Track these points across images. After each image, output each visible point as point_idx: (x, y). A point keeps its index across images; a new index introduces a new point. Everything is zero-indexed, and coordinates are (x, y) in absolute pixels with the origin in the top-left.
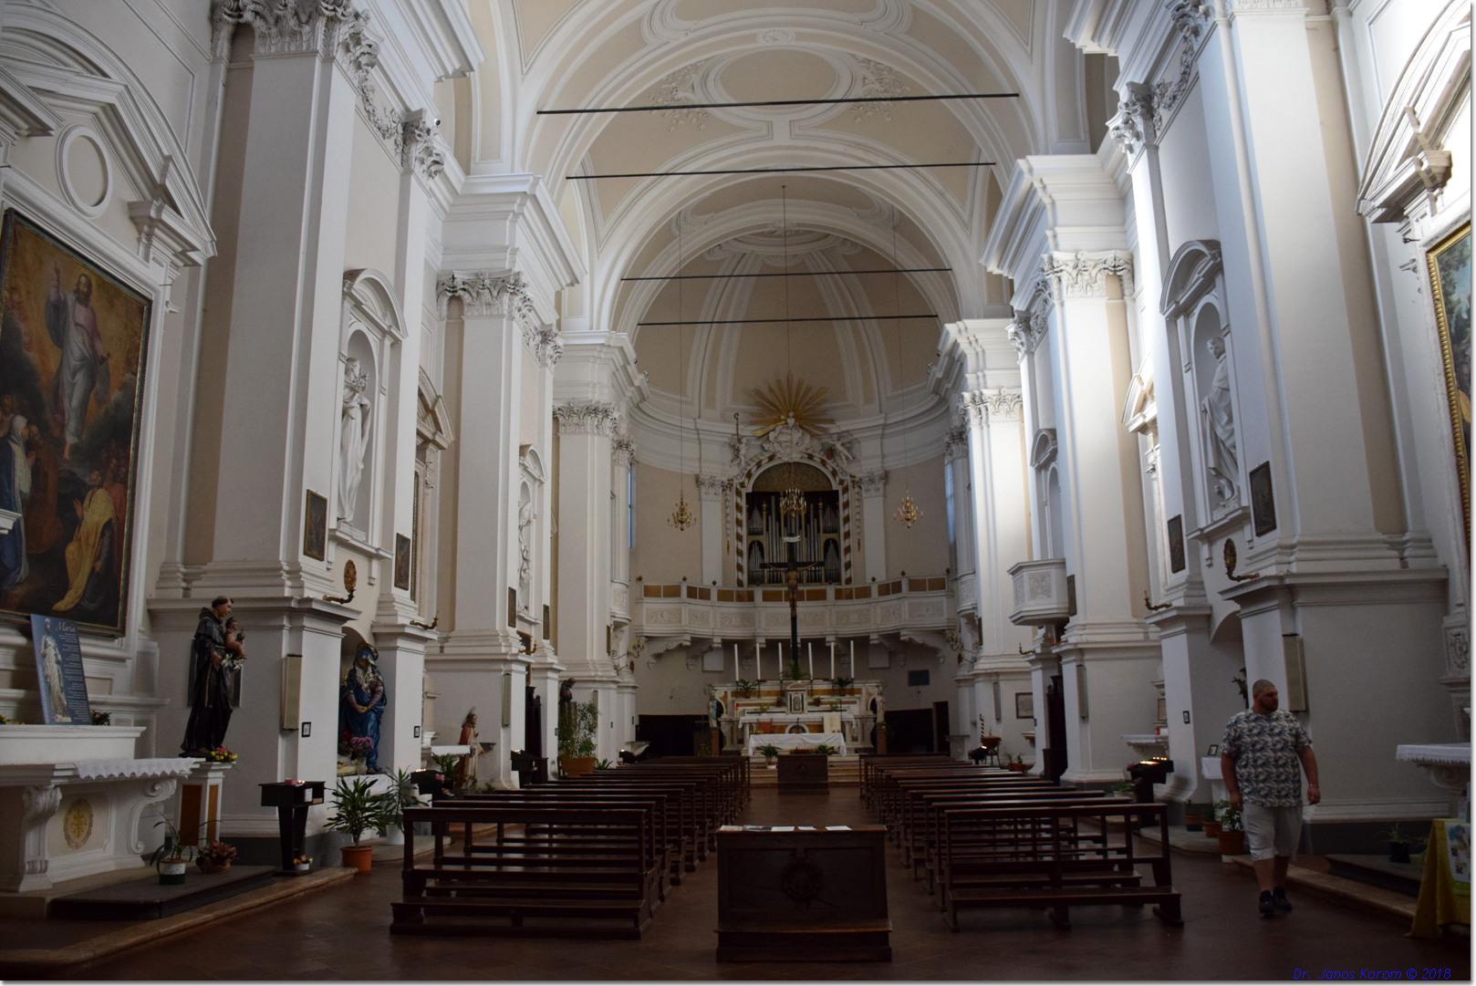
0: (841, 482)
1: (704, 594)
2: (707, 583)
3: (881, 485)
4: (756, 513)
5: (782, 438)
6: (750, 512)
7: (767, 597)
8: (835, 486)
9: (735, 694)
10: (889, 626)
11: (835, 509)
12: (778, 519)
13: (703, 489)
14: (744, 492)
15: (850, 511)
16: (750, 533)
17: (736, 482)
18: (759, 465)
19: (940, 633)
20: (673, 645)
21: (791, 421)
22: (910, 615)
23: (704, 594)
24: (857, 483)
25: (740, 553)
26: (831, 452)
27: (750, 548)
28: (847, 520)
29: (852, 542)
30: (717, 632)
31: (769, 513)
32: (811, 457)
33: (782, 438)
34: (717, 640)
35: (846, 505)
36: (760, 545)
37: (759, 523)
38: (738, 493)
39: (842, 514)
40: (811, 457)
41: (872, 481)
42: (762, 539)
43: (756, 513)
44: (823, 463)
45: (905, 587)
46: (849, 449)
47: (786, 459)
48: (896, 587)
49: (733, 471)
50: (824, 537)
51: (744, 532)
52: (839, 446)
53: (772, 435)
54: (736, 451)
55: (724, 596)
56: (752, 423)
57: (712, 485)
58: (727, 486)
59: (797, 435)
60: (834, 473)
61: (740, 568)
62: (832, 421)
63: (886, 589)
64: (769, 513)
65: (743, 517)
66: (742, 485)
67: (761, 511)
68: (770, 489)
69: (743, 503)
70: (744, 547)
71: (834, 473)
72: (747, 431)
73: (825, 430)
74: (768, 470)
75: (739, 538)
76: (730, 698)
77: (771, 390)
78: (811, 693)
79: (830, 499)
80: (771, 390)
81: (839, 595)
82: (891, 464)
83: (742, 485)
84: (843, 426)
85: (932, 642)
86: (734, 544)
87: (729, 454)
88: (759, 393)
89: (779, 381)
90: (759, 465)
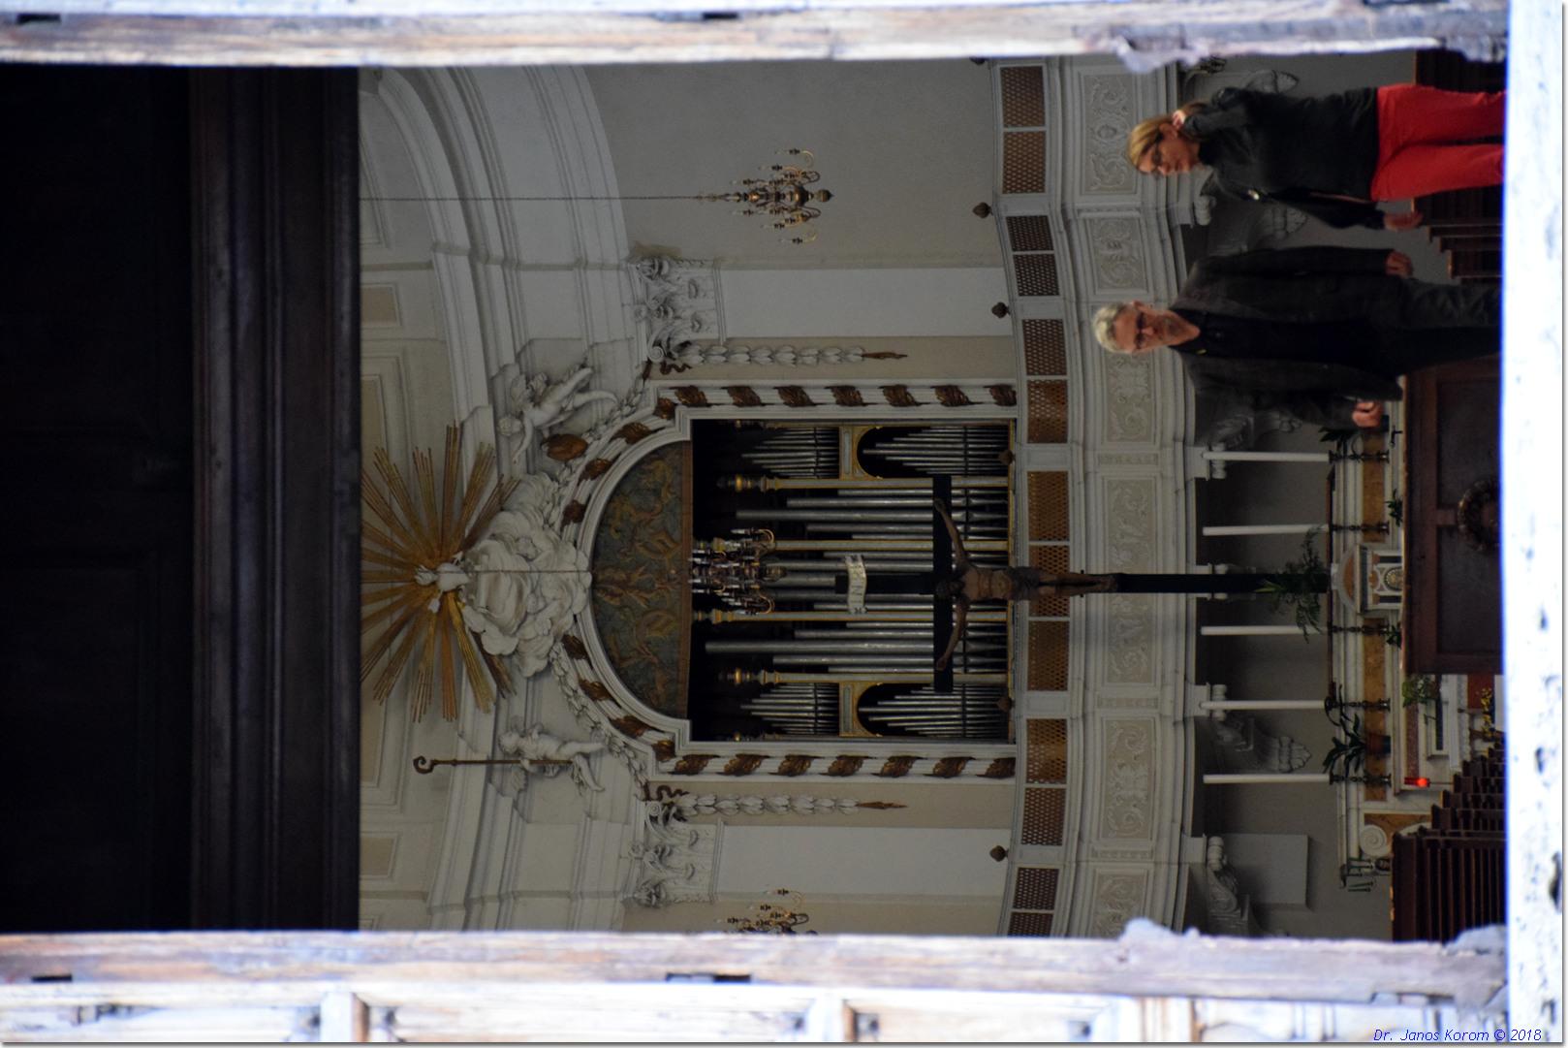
4: (764, 707)
8: (679, 431)
12: (785, 631)
14: (687, 747)
24: (671, 357)
26: (561, 443)
28: (795, 396)
31: (766, 662)
35: (744, 396)
36: (873, 695)
37: (797, 695)
38: (694, 765)
39: (775, 411)
43: (764, 707)
44: (597, 470)
47: (581, 599)
51: (828, 751)
52: (540, 416)
56: (452, 711)
64: (766, 662)
69: (727, 750)
86: (866, 782)
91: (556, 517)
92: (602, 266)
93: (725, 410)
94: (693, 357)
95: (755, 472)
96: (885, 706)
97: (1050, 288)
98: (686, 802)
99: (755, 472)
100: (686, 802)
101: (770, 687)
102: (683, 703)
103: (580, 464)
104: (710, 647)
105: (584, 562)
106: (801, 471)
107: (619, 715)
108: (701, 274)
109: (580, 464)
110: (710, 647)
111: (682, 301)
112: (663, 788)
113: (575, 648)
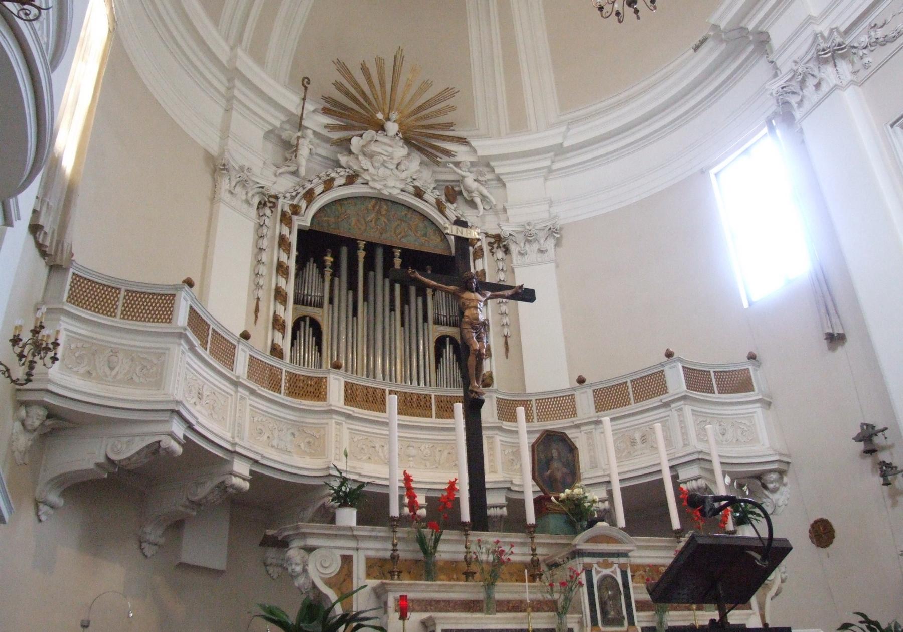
3: (550, 244)
5: (374, 148)
6: (301, 263)
12: (352, 285)
13: (225, 184)
16: (299, 301)
17: (284, 204)
20: (126, 448)
21: (392, 128)
26: (453, 193)
31: (336, 273)
32: (419, 193)
33: (374, 148)
34: (241, 468)
36: (316, 327)
37: (316, 288)
38: (286, 219)
41: (529, 238)
42: (323, 316)
43: (311, 269)
45: (676, 381)
48: (650, 385)
49: (283, 185)
50: (435, 331)
51: (290, 289)
52: (470, 181)
53: (356, 143)
54: (290, 148)
57: (243, 183)
58: (268, 202)
59: (401, 151)
62: (462, 141)
64: (336, 273)
65: (292, 265)
66: (296, 210)
67: (321, 267)
68: (344, 231)
69: (294, 239)
70: (288, 316)
72: (317, 122)
73: (448, 153)
75: (280, 296)
77: (365, 70)
82: (565, 215)
83: (296, 210)
84: (484, 147)
86: (269, 307)
88: (343, 68)
89: (380, 62)
90: (329, 184)
91: (417, 183)
94: (500, 254)
96: (309, 331)
100: (268, 212)
102: (316, 228)
103: (443, 198)
104: (344, 250)
105: (395, 192)
106: (437, 306)
110: (344, 250)
111: (536, 246)
112: (274, 205)
113: (351, 179)
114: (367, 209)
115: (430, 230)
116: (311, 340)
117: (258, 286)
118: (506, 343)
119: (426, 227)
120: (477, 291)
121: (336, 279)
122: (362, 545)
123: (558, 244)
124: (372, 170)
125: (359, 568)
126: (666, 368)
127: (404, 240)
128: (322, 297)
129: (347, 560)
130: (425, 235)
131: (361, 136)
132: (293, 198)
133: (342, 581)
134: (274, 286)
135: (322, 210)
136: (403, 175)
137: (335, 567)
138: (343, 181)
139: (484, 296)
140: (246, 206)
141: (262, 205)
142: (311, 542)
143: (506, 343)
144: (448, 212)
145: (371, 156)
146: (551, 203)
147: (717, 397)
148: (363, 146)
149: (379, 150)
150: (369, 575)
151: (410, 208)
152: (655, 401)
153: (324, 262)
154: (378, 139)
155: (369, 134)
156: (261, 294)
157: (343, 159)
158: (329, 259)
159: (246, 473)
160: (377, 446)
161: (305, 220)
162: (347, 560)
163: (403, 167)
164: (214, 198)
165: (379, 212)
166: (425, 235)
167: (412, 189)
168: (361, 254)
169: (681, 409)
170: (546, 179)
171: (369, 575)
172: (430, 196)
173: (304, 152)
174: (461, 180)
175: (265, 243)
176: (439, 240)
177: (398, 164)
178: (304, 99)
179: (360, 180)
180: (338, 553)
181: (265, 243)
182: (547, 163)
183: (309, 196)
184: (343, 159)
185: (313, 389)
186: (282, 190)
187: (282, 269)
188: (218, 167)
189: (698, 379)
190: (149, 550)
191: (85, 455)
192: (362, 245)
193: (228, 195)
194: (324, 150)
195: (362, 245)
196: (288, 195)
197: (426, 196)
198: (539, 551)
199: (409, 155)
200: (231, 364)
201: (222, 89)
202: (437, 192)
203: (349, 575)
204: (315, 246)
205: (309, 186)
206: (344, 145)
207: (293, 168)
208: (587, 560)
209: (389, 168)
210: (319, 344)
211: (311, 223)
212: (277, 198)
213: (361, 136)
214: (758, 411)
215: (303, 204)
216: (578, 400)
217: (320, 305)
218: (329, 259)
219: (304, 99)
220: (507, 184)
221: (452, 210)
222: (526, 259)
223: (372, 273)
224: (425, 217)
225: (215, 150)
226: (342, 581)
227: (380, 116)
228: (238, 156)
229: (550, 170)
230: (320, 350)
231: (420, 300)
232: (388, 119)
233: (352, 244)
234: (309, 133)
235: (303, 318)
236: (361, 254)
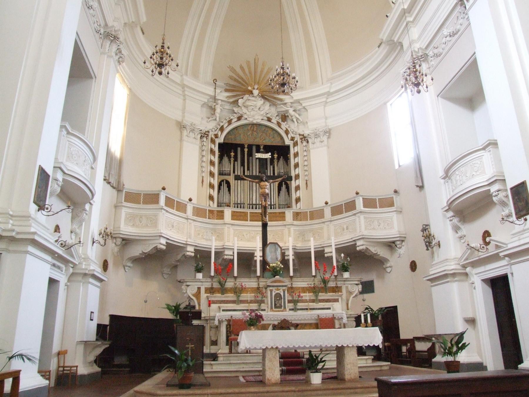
0: (292, 139)
1: (181, 207)
2: (184, 198)
3: (325, 138)
4: (226, 159)
5: (248, 103)
6: (221, 158)
7: (235, 216)
8: (288, 142)
9: (211, 290)
10: (345, 238)
11: (287, 160)
12: (243, 164)
13: (185, 133)
14: (218, 141)
15: (299, 160)
16: (221, 173)
17: (211, 135)
18: (230, 122)
19: (391, 245)
20: (148, 248)
21: (256, 92)
22: (365, 229)
23: (181, 207)
24: (304, 138)
25: (211, 186)
26: (284, 117)
27: (220, 185)
28: (297, 166)
29: (300, 182)
30: (190, 241)
31: (236, 160)
33: (248, 103)
34: (191, 249)
35: (296, 155)
36: (228, 183)
37: (228, 166)
38: (213, 141)
39: (292, 162)
40: (269, 120)
41: (317, 136)
43: (226, 159)
44: (279, 124)
45: (360, 204)
46: (299, 115)
47: (251, 120)
48: (350, 206)
49: (210, 126)
51: (216, 171)
52: (291, 112)
53: (240, 101)
54: (213, 110)
55: (199, 212)
56: (227, 90)
57: (193, 130)
58: (204, 135)
59: (260, 102)
60: (287, 132)
61: (211, 198)
63: (337, 210)
64: (236, 160)
65: (216, 160)
66: (216, 136)
67: (229, 157)
69: (216, 149)
71: (287, 132)
72: (223, 95)
73: (281, 100)
74: (236, 128)
75: (212, 174)
76: (204, 295)
77: (242, 68)
78: (291, 290)
79: (282, 152)
80: (242, 68)
81: (297, 216)
82: (331, 123)
83: (216, 136)
85: (382, 252)
86: (208, 179)
87: (205, 112)
88: (233, 70)
89: (248, 63)
90: (230, 122)
91: (268, 116)
92: (326, 122)
93: (292, 151)
94: (305, 143)
95: (278, 159)
96: (225, 185)
97: (333, 214)
98: (205, 139)
99: (278, 159)
100: (205, 139)
101: (230, 161)
102: (226, 141)
103: (280, 121)
104: (239, 149)
105: (259, 121)
106: (279, 169)
107: (225, 127)
108: (326, 142)
109: (280, 121)
110: (239, 149)
111: (319, 139)
112: (208, 135)
113: (239, 119)
114: (248, 130)
115: (276, 135)
116: (226, 189)
117: (203, 172)
118: (307, 183)
119: (274, 134)
120: (266, 181)
121: (236, 162)
122: (204, 284)
123: (329, 137)
124: (248, 113)
125: (203, 290)
126: (356, 199)
127: (264, 141)
128: (230, 171)
129: (199, 288)
130: (273, 138)
131: (243, 98)
132: (216, 130)
133: (198, 295)
134: (209, 170)
135: (229, 133)
136: (262, 113)
137: (195, 290)
138: (236, 120)
139: (268, 182)
140: (195, 140)
141: (201, 137)
142: (188, 284)
143: (307, 183)
144: (282, 127)
145: (246, 107)
146: (326, 118)
147: (379, 210)
148: (244, 103)
149: (250, 104)
150: (206, 293)
151: (266, 126)
152: (350, 213)
153: (231, 155)
154: (250, 98)
155: (246, 97)
156: (203, 174)
157: (236, 110)
158: (232, 154)
159: (193, 250)
160: (245, 234)
161: (221, 140)
162: (199, 288)
163: (261, 109)
164: (181, 140)
165: (253, 130)
166: (273, 138)
167: (266, 119)
168: (246, 150)
169: (359, 217)
170: (325, 106)
171: (206, 293)
172: (274, 120)
173: (218, 110)
174: (287, 111)
175: (204, 153)
176: (279, 139)
177: (259, 108)
178: (215, 88)
179: (243, 118)
180: (196, 287)
181: (204, 153)
182: (324, 100)
183: (222, 129)
184: (236, 110)
185: (220, 215)
186: (211, 128)
187: (212, 163)
188: (181, 126)
189: (369, 203)
190: (165, 276)
191: (137, 251)
192: (246, 146)
193: (187, 137)
194: (228, 107)
195: (246, 146)
196: (213, 130)
197: (272, 121)
198: (261, 284)
199: (264, 103)
200: (185, 212)
201: (181, 92)
202: (278, 118)
203: (200, 293)
204: (226, 149)
205: (222, 124)
206: (236, 103)
207: (214, 118)
208: (271, 288)
209: (256, 110)
210: (229, 190)
211: (224, 140)
212: (209, 132)
213: (243, 98)
214: (394, 216)
215: (219, 133)
216: (325, 210)
217: (230, 175)
218: (232, 154)
219: (215, 88)
220: (308, 110)
221: (284, 125)
222: (315, 146)
223: (251, 158)
224: (273, 130)
225: (179, 119)
226: (198, 295)
227: (250, 88)
228: (188, 120)
229: (326, 103)
230: (230, 193)
231: (272, 167)
232: (254, 89)
233: (242, 146)
234: (219, 102)
235: (223, 181)
236: (246, 150)
